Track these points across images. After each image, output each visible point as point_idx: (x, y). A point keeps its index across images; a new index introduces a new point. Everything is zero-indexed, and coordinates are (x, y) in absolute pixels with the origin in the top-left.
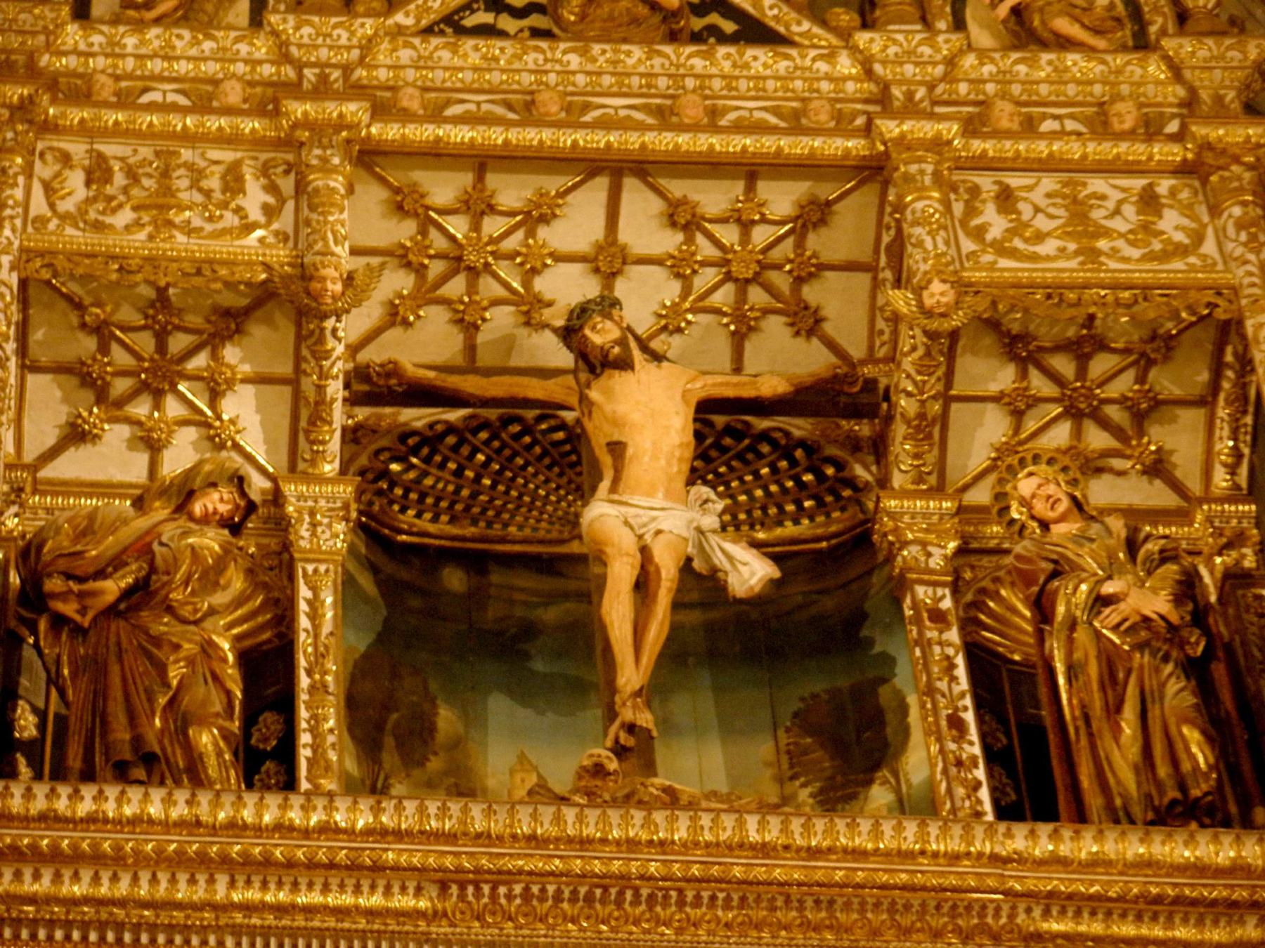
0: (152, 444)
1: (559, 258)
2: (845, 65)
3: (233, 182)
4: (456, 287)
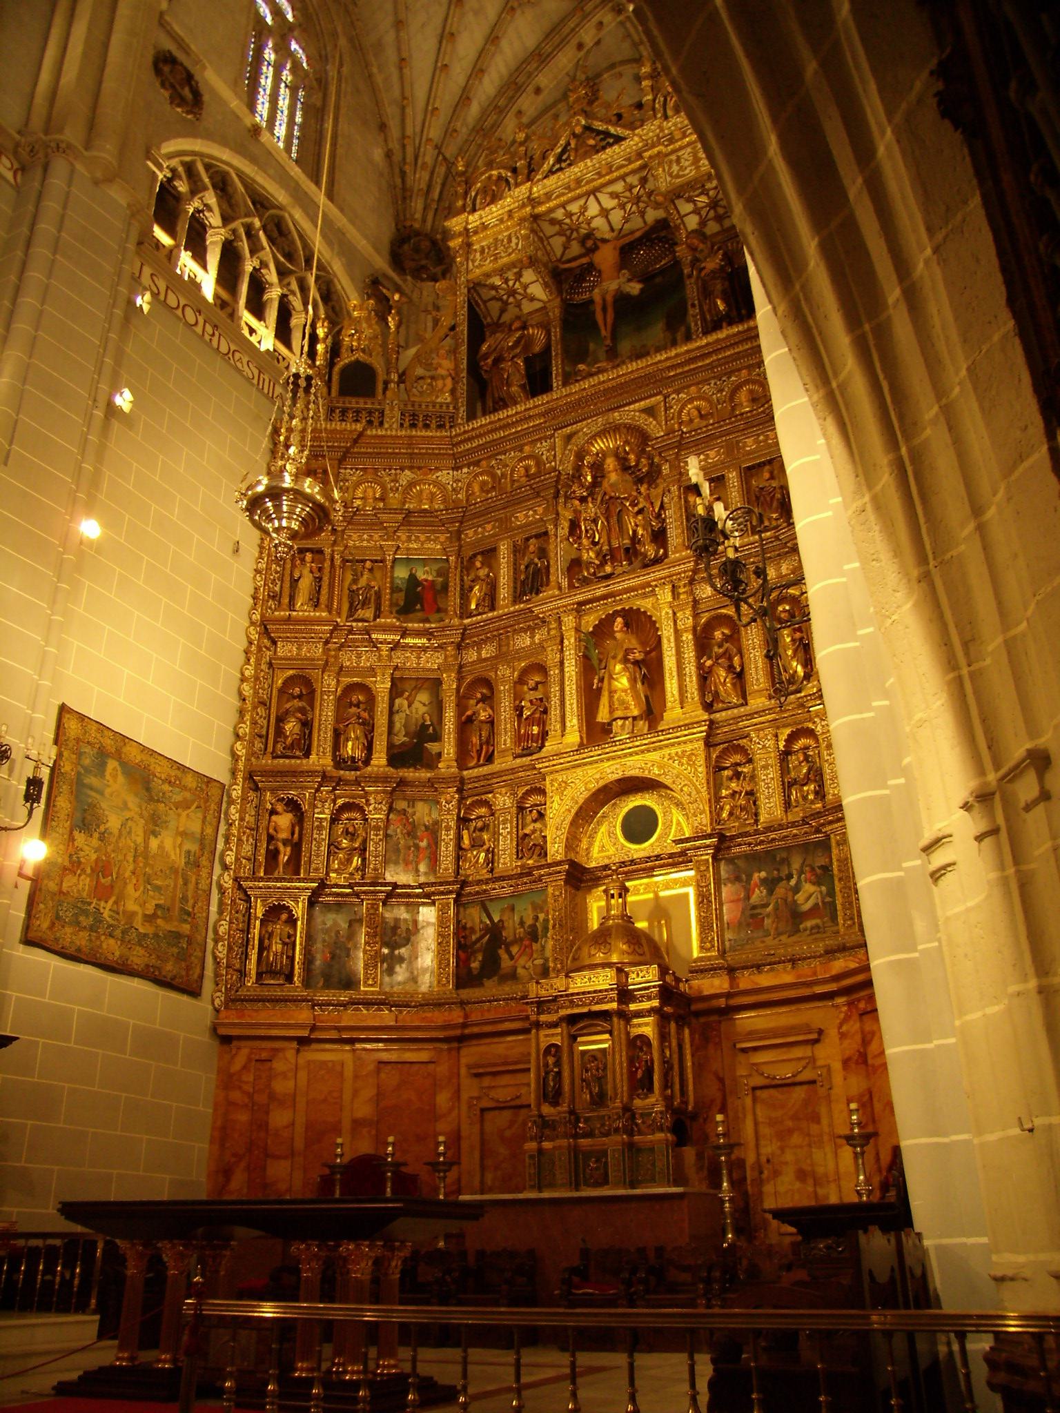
0: (519, 305)
1: (592, 218)
2: (636, 139)
3: (510, 241)
4: (575, 235)
